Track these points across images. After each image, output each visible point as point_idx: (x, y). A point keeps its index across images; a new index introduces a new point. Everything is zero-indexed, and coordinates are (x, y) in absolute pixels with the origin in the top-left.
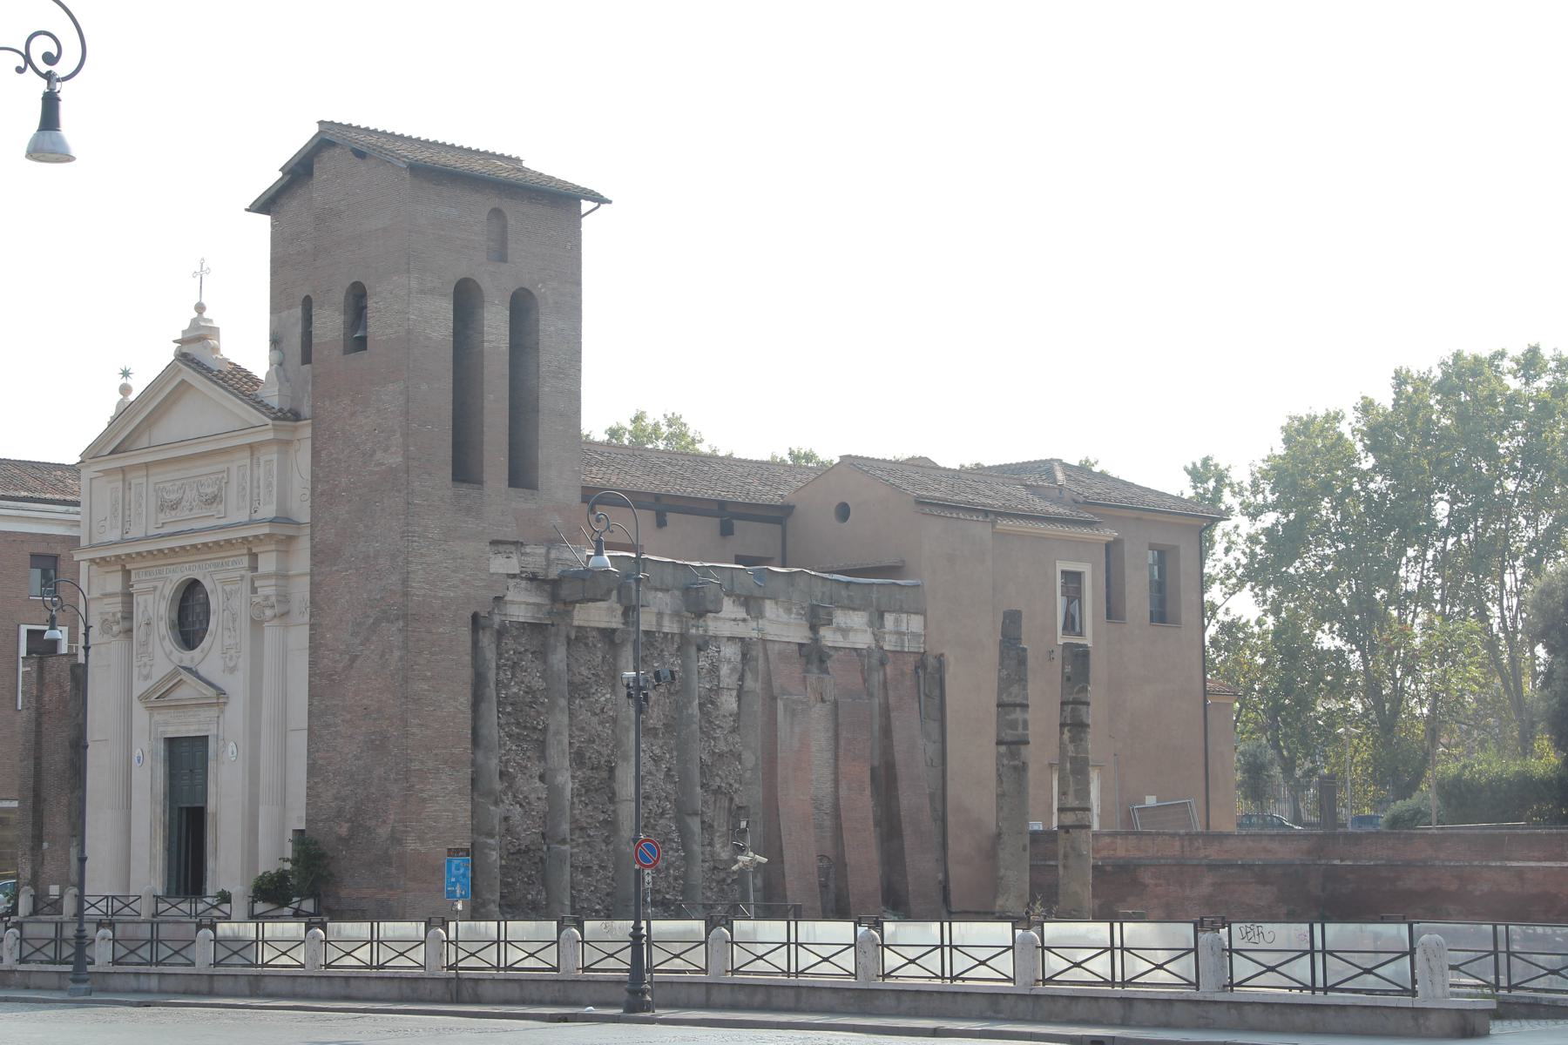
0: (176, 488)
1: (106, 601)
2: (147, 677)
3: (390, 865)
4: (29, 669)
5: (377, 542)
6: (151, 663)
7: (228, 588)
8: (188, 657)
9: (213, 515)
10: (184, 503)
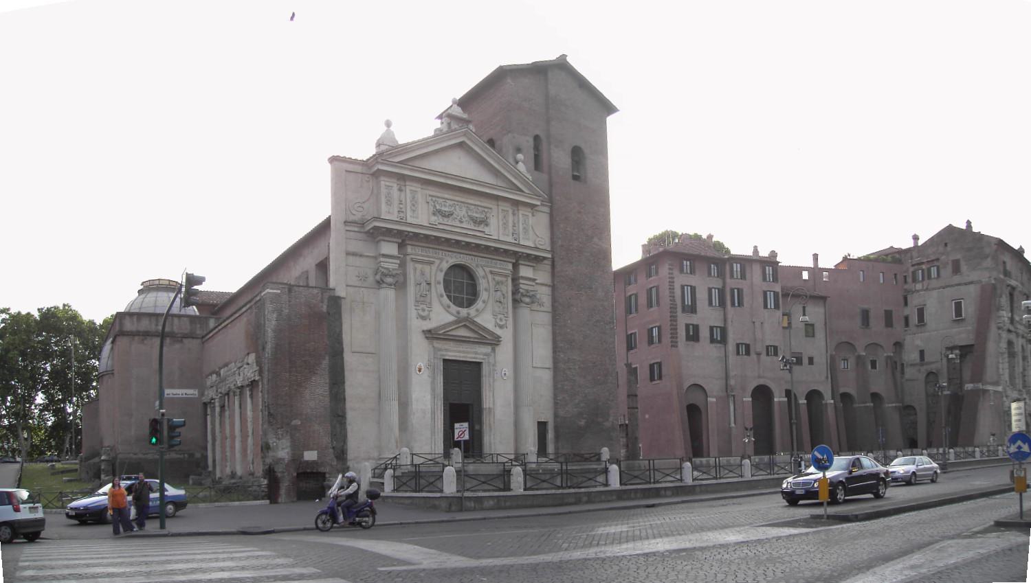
0: (448, 204)
1: (382, 259)
2: (424, 318)
6: (429, 309)
7: (498, 278)
8: (464, 312)
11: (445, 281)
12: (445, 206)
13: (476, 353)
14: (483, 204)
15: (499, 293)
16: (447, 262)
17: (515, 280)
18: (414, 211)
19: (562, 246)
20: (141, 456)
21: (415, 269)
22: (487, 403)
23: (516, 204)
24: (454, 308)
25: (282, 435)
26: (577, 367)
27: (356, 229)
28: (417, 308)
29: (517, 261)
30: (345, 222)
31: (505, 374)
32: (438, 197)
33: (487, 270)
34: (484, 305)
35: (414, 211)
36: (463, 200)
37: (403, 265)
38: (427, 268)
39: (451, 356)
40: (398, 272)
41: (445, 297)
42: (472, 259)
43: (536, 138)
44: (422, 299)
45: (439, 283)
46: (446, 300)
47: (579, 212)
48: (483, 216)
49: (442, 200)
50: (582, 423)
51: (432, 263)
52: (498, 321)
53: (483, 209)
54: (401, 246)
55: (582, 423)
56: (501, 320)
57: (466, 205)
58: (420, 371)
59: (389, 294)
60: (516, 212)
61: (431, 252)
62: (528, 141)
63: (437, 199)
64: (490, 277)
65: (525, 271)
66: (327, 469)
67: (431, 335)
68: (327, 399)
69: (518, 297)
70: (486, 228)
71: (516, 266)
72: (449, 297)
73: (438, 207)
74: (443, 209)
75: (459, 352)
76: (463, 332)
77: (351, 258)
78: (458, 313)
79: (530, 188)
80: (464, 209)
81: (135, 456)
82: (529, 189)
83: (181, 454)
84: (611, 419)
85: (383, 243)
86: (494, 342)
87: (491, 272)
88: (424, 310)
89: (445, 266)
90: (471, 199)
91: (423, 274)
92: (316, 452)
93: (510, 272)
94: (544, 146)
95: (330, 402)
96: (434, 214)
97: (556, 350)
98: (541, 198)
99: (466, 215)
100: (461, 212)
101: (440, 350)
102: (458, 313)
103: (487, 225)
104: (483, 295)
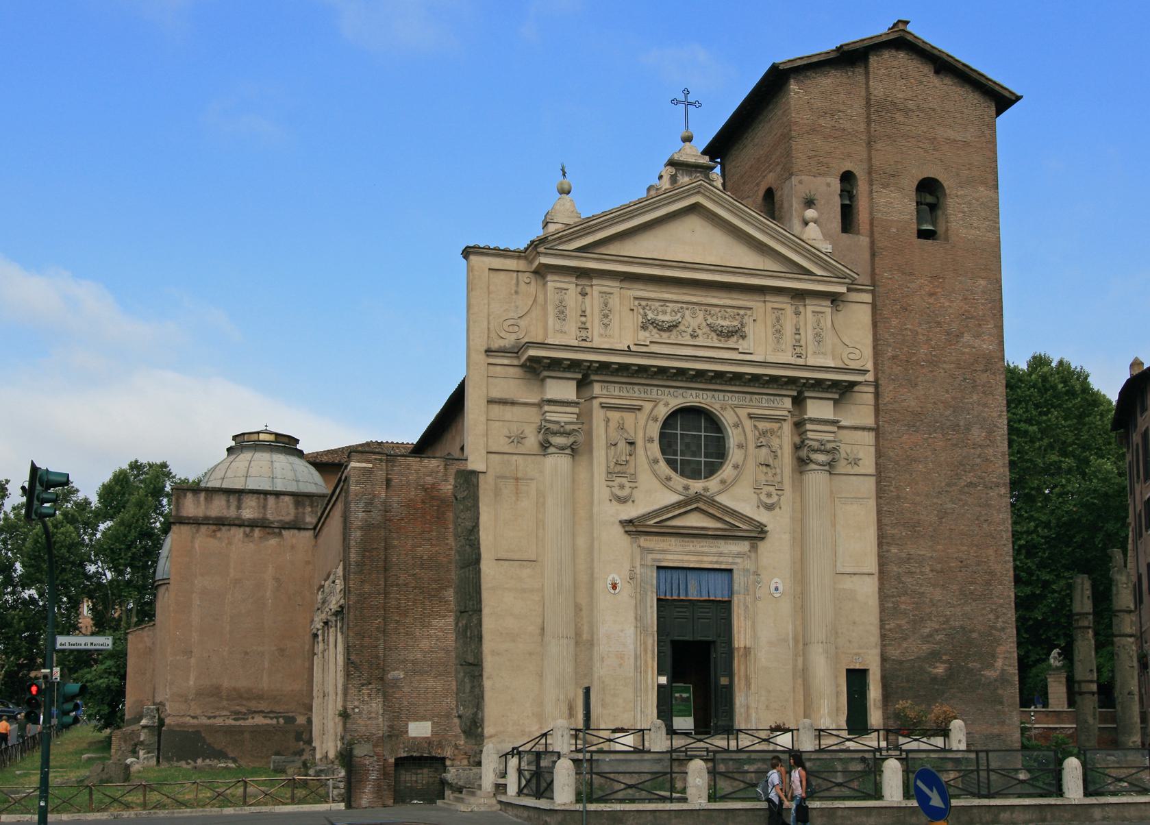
0: (669, 310)
1: (546, 408)
2: (622, 500)
3: (1001, 703)
4: (371, 465)
5: (969, 414)
6: (633, 485)
7: (762, 425)
8: (697, 486)
9: (738, 349)
10: (681, 327)
11: (662, 435)
12: (665, 313)
13: (721, 554)
14: (734, 303)
15: (764, 451)
16: (667, 404)
17: (799, 425)
18: (606, 325)
19: (894, 357)
20: (205, 721)
21: (607, 420)
22: (741, 638)
23: (800, 295)
24: (678, 481)
25: (369, 695)
26: (928, 569)
27: (506, 361)
28: (611, 484)
29: (800, 393)
30: (486, 351)
31: (777, 589)
32: (653, 300)
33: (743, 413)
34: (735, 472)
35: (606, 325)
36: (694, 299)
37: (585, 417)
38: (629, 417)
39: (671, 560)
40: (576, 427)
41: (662, 464)
42: (713, 396)
43: (847, 178)
44: (618, 468)
45: (651, 440)
46: (664, 468)
47: (931, 295)
48: (735, 323)
49: (657, 304)
50: (940, 670)
51: (639, 409)
52: (764, 498)
53: (736, 311)
54: (583, 384)
55: (940, 670)
56: (769, 495)
57: (703, 308)
58: (614, 586)
59: (558, 463)
60: (801, 309)
61: (636, 392)
62: (828, 185)
63: (649, 303)
64: (748, 424)
65: (818, 409)
66: (448, 752)
67: (634, 528)
68: (452, 637)
69: (804, 453)
70: (741, 341)
71: (798, 401)
72: (671, 463)
73: (650, 316)
74: (661, 317)
75: (688, 553)
76: (695, 521)
77: (496, 410)
78: (687, 488)
79: (825, 265)
80: (701, 315)
81: (192, 721)
82: (825, 269)
83: (272, 718)
84: (999, 663)
85: (548, 381)
86: (758, 534)
87: (751, 416)
88: (622, 487)
89: (663, 412)
90: (713, 297)
91: (621, 427)
92: (429, 724)
93: (786, 413)
94: (862, 188)
95: (456, 641)
96: (644, 328)
97: (883, 540)
98: (847, 281)
99: (704, 324)
100: (693, 320)
101: (650, 551)
102: (687, 488)
103: (743, 337)
104: (735, 455)
